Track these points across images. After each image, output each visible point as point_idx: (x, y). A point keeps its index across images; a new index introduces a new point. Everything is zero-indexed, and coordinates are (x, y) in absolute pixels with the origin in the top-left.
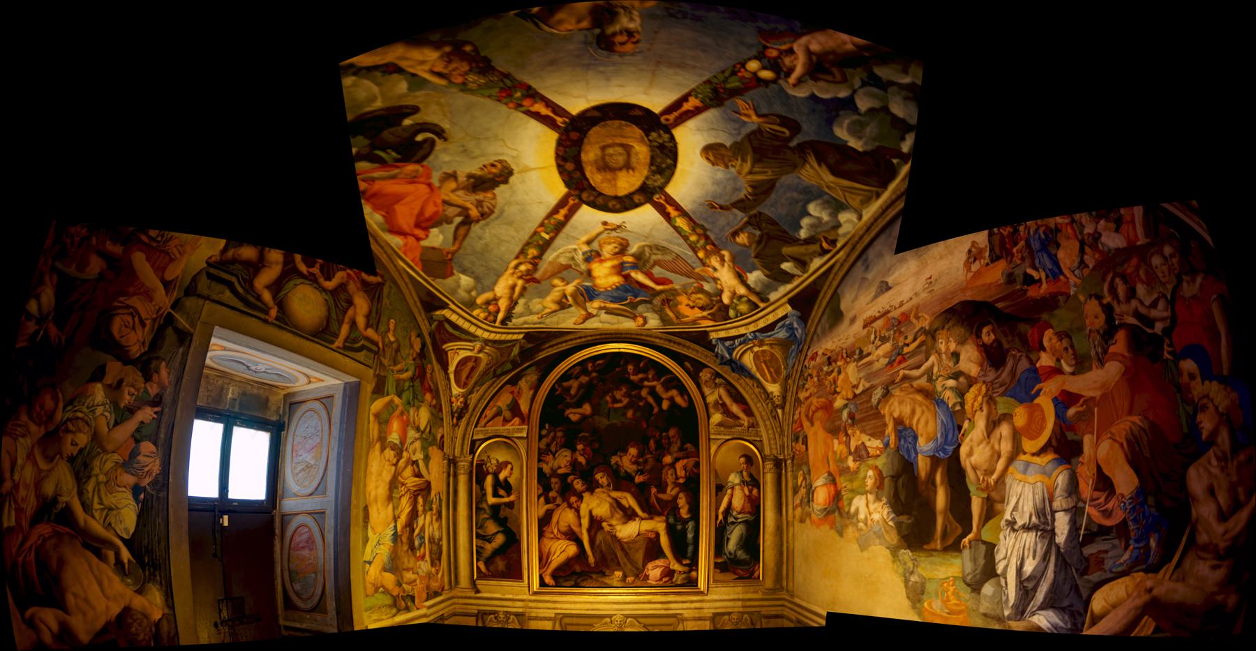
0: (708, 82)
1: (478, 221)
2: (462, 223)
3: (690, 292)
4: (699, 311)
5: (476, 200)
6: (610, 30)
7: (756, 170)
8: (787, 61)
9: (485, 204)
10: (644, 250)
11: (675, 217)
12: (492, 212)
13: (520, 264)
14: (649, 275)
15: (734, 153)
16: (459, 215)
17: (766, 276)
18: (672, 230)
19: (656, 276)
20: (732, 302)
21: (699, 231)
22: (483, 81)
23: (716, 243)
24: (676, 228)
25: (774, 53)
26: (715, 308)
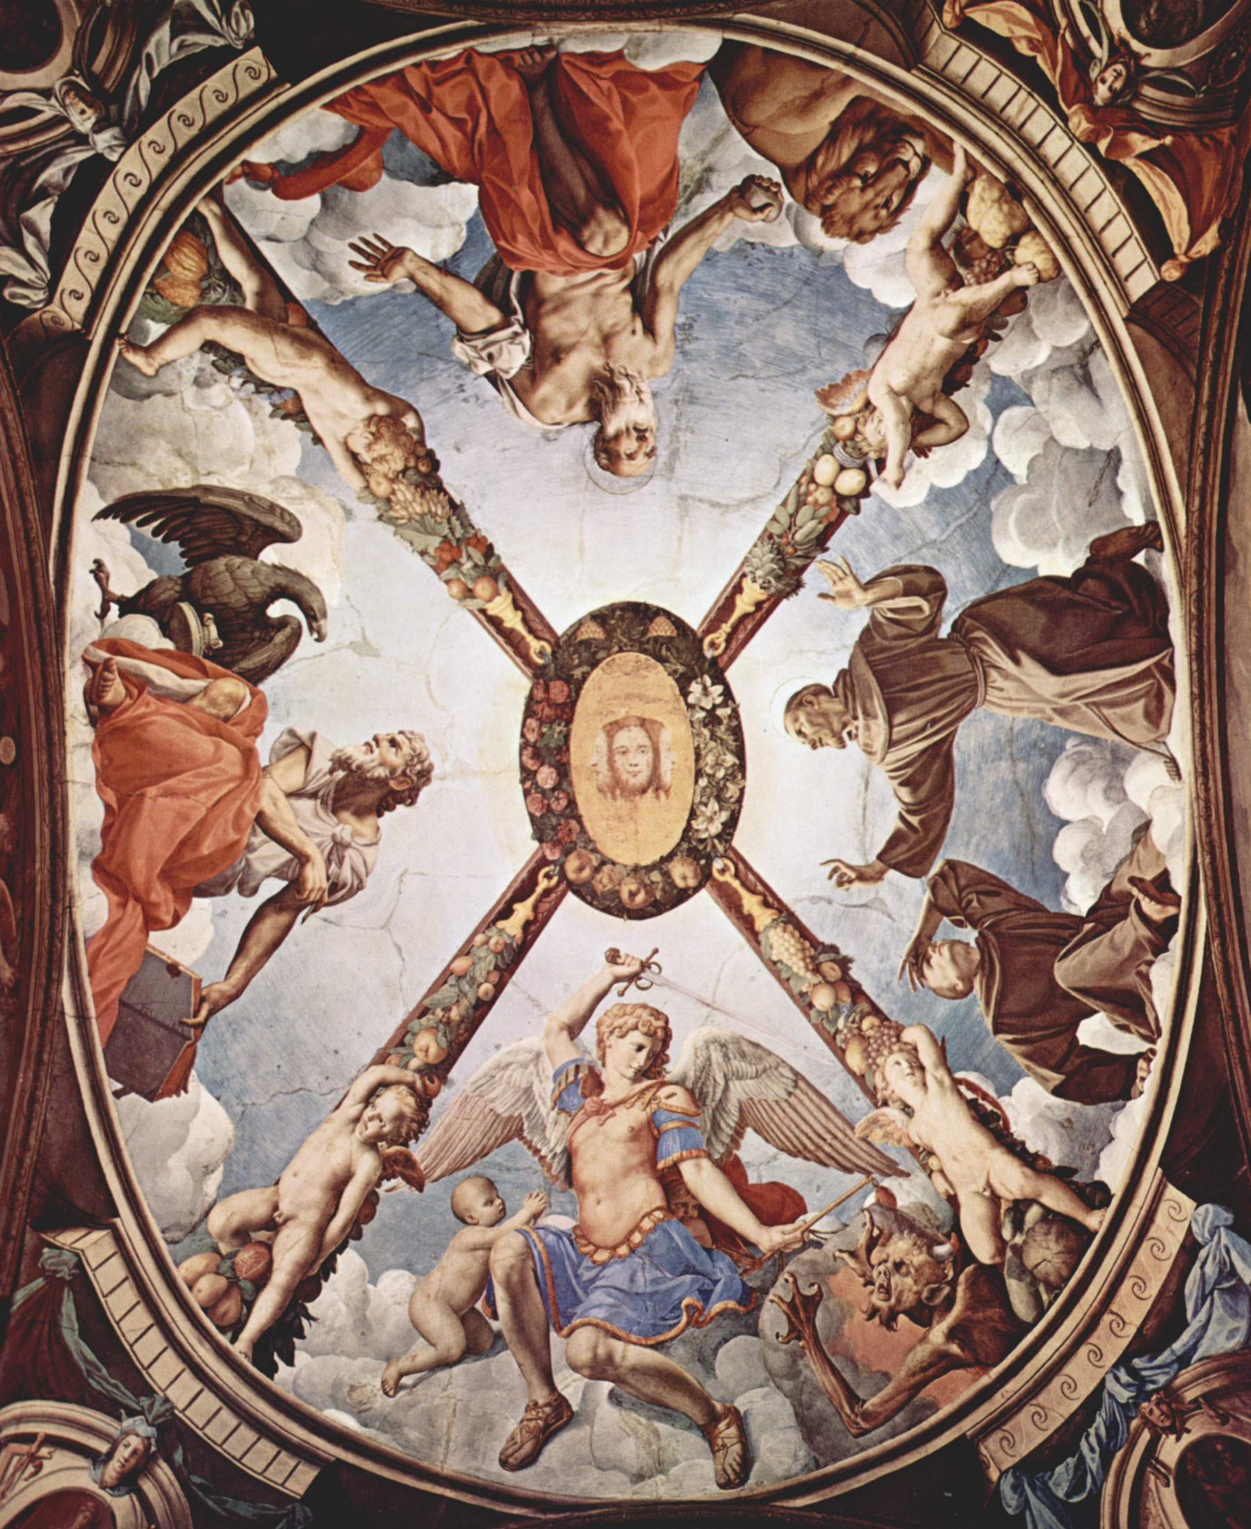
0: (767, 536)
1: (317, 905)
2: (275, 903)
3: (862, 1239)
4: (921, 1330)
5: (334, 837)
6: (611, 430)
7: (898, 732)
8: (869, 431)
9: (349, 853)
10: (709, 1059)
11: (767, 928)
12: (360, 887)
13: (384, 1085)
14: (732, 1170)
15: (846, 705)
16: (279, 873)
17: (1057, 1092)
18: (767, 977)
19: (753, 1179)
20: (1001, 1246)
21: (832, 971)
22: (418, 509)
23: (882, 1005)
24: (773, 966)
25: (845, 427)
26: (960, 1291)
